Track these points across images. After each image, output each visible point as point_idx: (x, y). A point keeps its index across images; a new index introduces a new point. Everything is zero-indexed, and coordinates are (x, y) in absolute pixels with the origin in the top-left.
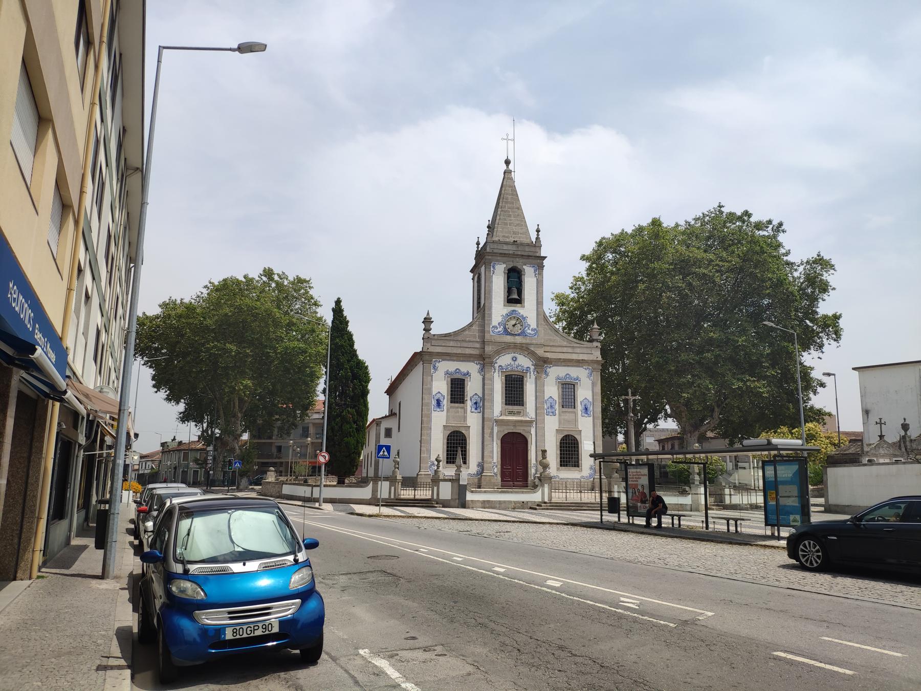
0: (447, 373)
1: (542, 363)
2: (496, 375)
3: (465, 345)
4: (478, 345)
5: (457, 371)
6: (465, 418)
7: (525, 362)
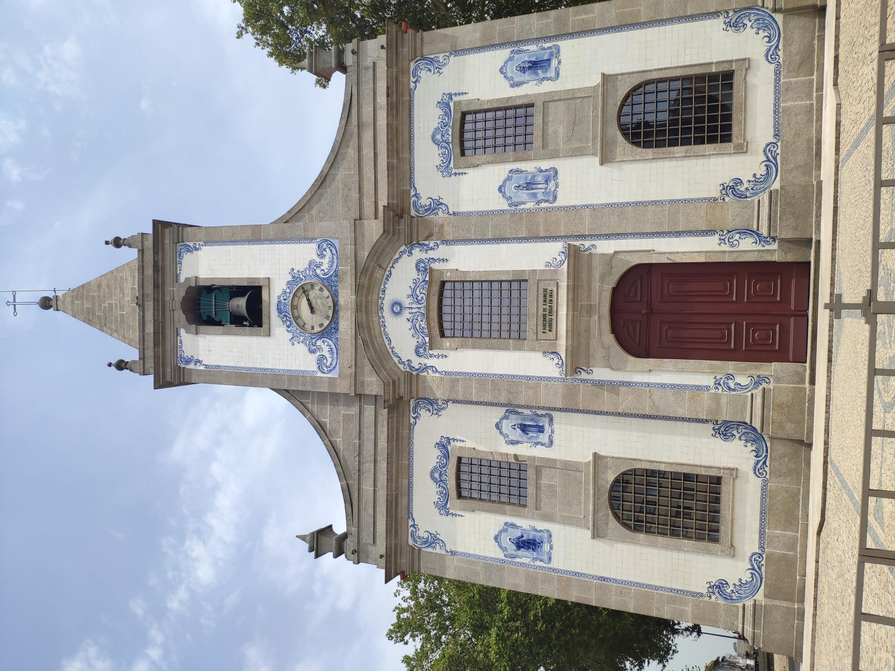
1: (403, 226)
3: (368, 447)
4: (369, 410)
7: (402, 279)
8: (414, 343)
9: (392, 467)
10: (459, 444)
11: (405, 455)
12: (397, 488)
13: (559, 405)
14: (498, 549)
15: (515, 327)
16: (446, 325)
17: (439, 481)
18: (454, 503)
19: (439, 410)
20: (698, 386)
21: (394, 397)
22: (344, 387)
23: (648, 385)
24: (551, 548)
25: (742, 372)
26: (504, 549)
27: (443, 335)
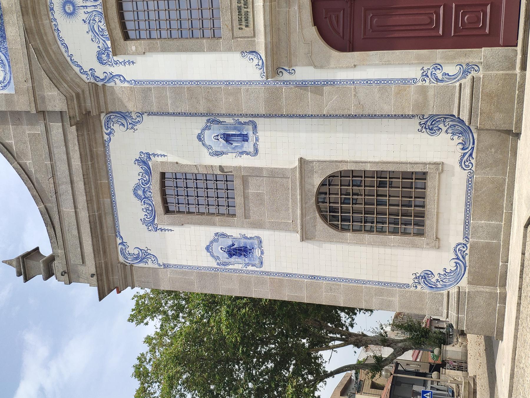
0: (150, 223)
2: (130, 72)
5: (141, 192)
6: (275, 175)
8: (94, 48)
9: (90, 188)
10: (160, 159)
11: (104, 173)
12: (99, 209)
13: (262, 111)
14: (211, 259)
15: (207, 24)
16: (130, 25)
17: (144, 198)
18: (161, 218)
19: (134, 124)
20: (405, 80)
21: (80, 113)
22: (23, 104)
23: (353, 81)
24: (262, 253)
25: (449, 60)
26: (216, 258)
27: (126, 37)
